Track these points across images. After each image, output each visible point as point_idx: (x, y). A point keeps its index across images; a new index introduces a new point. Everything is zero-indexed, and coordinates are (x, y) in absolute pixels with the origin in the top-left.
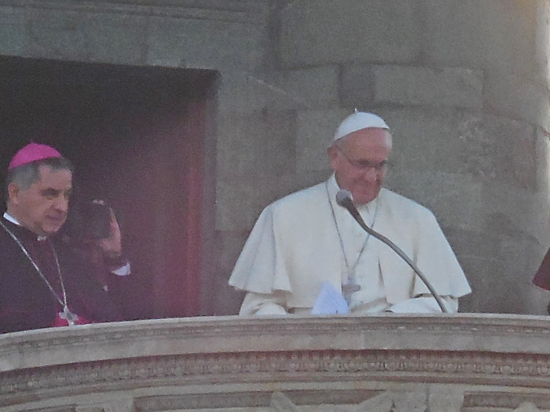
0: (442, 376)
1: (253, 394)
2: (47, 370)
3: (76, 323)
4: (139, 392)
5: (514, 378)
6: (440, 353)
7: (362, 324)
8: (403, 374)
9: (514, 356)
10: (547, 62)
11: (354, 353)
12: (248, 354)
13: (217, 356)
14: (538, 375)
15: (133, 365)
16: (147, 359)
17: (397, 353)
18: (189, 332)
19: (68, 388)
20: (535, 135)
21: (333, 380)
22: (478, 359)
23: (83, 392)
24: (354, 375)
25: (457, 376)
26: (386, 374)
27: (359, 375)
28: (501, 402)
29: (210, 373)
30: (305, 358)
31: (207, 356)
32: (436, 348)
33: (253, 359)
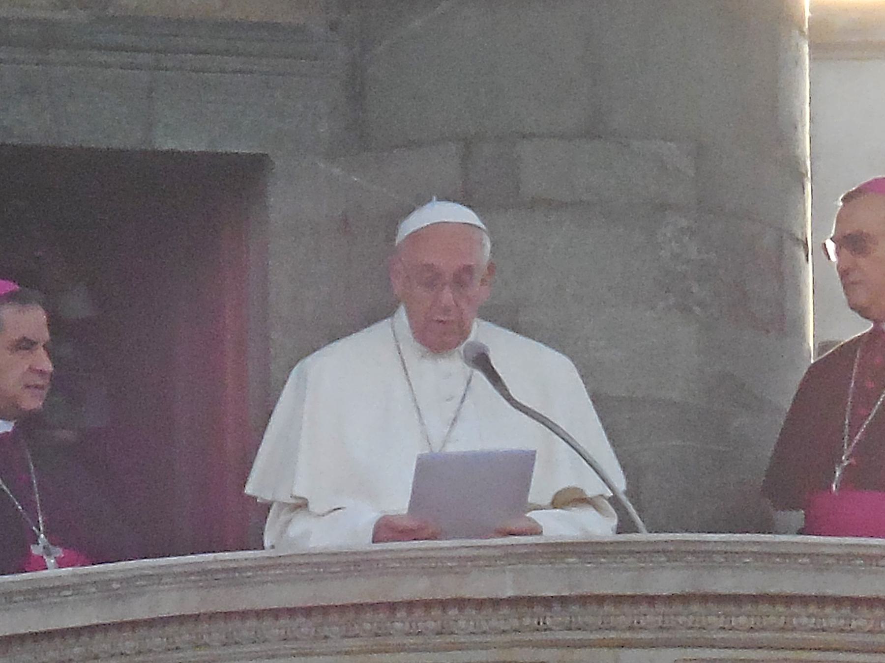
3: (60, 564)
5: (756, 635)
6: (634, 600)
7: (507, 556)
8: (578, 635)
9: (756, 599)
11: (496, 603)
12: (325, 610)
13: (276, 613)
14: (794, 629)
15: (142, 632)
16: (166, 621)
17: (563, 600)
22: (695, 608)
24: (501, 639)
25: (665, 635)
29: (296, 639)
30: (419, 613)
31: (259, 614)
33: (334, 617)
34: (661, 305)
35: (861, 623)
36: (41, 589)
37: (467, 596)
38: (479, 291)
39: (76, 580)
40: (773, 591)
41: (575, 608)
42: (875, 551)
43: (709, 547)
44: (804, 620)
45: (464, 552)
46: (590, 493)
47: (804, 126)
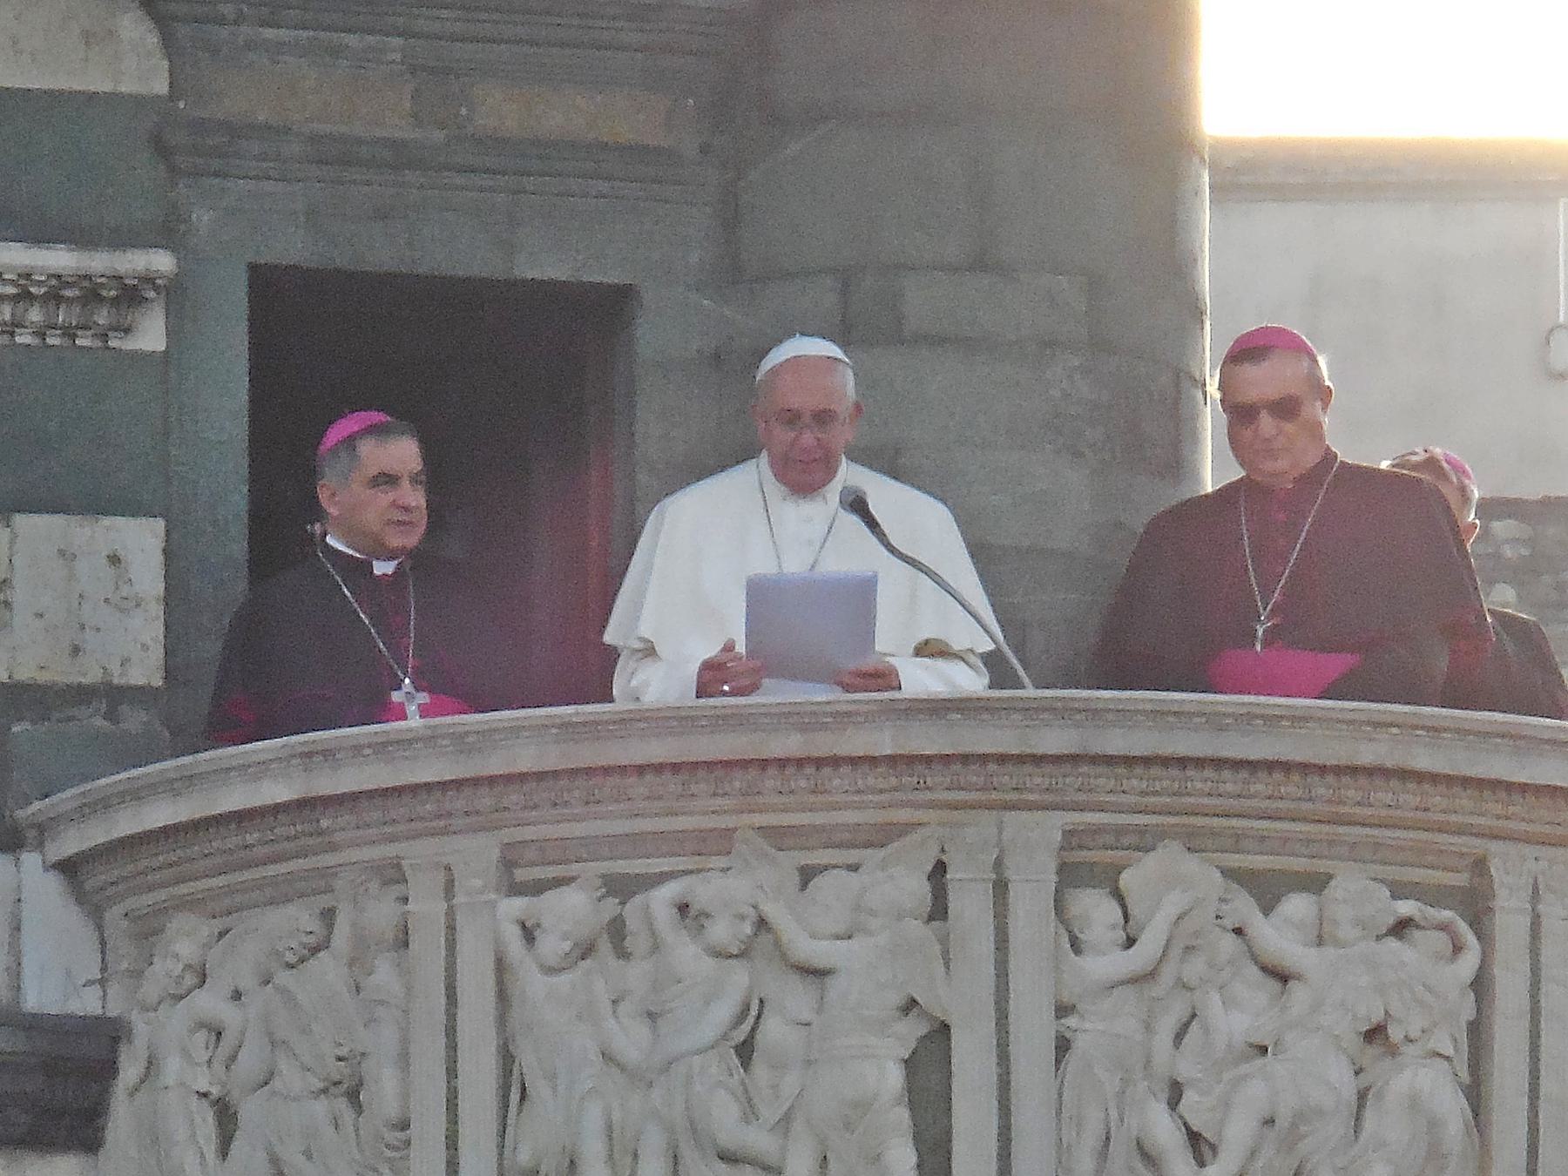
1: (702, 835)
2: (355, 797)
4: (509, 835)
6: (1021, 759)
9: (1147, 761)
10: (1195, 260)
11: (873, 761)
12: (695, 765)
13: (641, 770)
14: (1189, 794)
16: (522, 777)
17: (946, 759)
18: (592, 728)
19: (388, 829)
20: (1177, 385)
23: (417, 836)
24: (876, 798)
25: (1049, 798)
26: (928, 796)
28: (1126, 841)
30: (790, 770)
31: (623, 770)
33: (701, 773)
35: (1260, 787)
36: (391, 743)
38: (843, 434)
39: (429, 732)
41: (957, 767)
43: (1100, 706)
44: (1199, 785)
45: (845, 708)
46: (957, 645)
47: (1204, 260)
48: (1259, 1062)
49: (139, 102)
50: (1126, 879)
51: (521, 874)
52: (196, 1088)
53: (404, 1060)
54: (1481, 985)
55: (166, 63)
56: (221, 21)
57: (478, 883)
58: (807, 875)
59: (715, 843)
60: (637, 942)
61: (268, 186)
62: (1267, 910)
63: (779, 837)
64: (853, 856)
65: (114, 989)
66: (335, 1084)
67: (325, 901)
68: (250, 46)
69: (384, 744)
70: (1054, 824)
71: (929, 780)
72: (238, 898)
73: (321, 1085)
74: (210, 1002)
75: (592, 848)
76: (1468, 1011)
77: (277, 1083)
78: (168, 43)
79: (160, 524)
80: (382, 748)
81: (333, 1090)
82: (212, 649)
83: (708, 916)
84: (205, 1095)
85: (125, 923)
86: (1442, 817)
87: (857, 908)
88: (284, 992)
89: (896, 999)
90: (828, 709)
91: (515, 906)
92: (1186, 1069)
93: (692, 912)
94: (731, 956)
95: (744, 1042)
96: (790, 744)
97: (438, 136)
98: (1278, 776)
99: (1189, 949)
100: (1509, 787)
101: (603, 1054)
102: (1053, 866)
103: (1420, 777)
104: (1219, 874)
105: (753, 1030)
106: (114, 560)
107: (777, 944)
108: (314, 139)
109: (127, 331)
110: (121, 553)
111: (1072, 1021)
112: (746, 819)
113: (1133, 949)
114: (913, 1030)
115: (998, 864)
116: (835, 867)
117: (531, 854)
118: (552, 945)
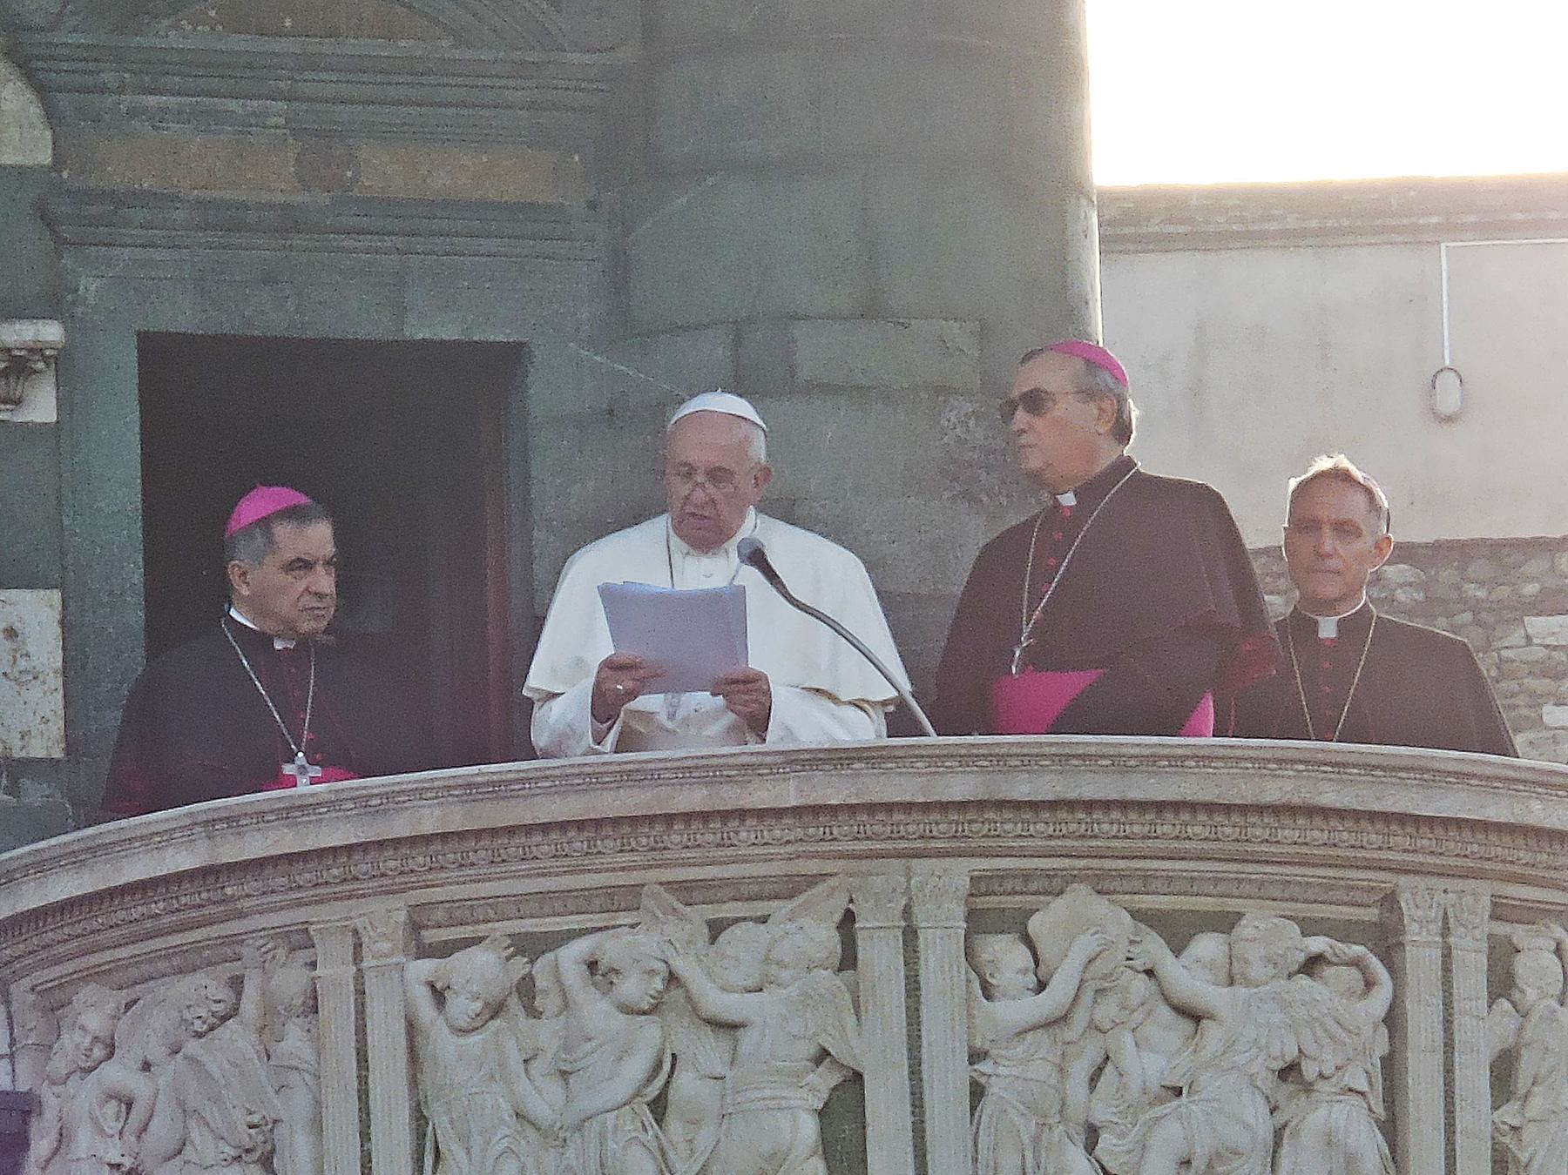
0: (933, 844)
1: (610, 891)
2: (259, 864)
3: (314, 781)
5: (1053, 843)
6: (927, 807)
9: (1054, 805)
11: (778, 813)
12: (598, 823)
13: (546, 828)
16: (427, 839)
17: (852, 809)
18: (498, 790)
21: (745, 860)
22: (991, 815)
25: (955, 844)
26: (836, 846)
27: (790, 848)
28: (1034, 886)
31: (529, 829)
32: (921, 800)
34: (947, 494)
37: (748, 806)
40: (1072, 795)
42: (1180, 752)
48: (1176, 1103)
49: (21, 172)
50: (1035, 925)
51: (430, 936)
52: (107, 1160)
53: (317, 1125)
54: (1393, 1019)
55: (48, 134)
56: (103, 90)
57: (386, 946)
58: (716, 929)
59: (623, 899)
60: (548, 1002)
61: (158, 255)
62: (1177, 951)
63: (686, 891)
64: (760, 908)
65: (24, 1064)
66: (248, 1151)
67: (234, 968)
68: (133, 113)
69: (288, 809)
70: (961, 872)
71: (835, 831)
72: (146, 969)
73: (233, 1153)
74: (117, 1074)
75: (498, 908)
76: (1382, 1048)
77: (189, 1152)
78: (52, 116)
79: (56, 595)
80: (288, 814)
81: (245, 1158)
82: (113, 718)
83: (617, 972)
84: (119, 1166)
85: (32, 997)
86: (1351, 853)
87: (767, 960)
88: (191, 1059)
89: (807, 1049)
90: (732, 761)
91: (425, 968)
92: (1101, 1113)
93: (602, 968)
94: (644, 1013)
95: (659, 1096)
96: (693, 798)
97: (324, 198)
98: (1186, 816)
99: (1100, 992)
100: (1417, 820)
101: (517, 1114)
102: (960, 911)
103: (1325, 812)
104: (1126, 916)
105: (667, 1083)
106: (11, 633)
107: (689, 998)
108: (201, 204)
109: (18, 402)
110: (17, 626)
111: (985, 1067)
112: (653, 875)
113: (1044, 993)
114: (825, 1081)
115: (907, 912)
116: (744, 919)
117: (439, 915)
118: (462, 1006)
